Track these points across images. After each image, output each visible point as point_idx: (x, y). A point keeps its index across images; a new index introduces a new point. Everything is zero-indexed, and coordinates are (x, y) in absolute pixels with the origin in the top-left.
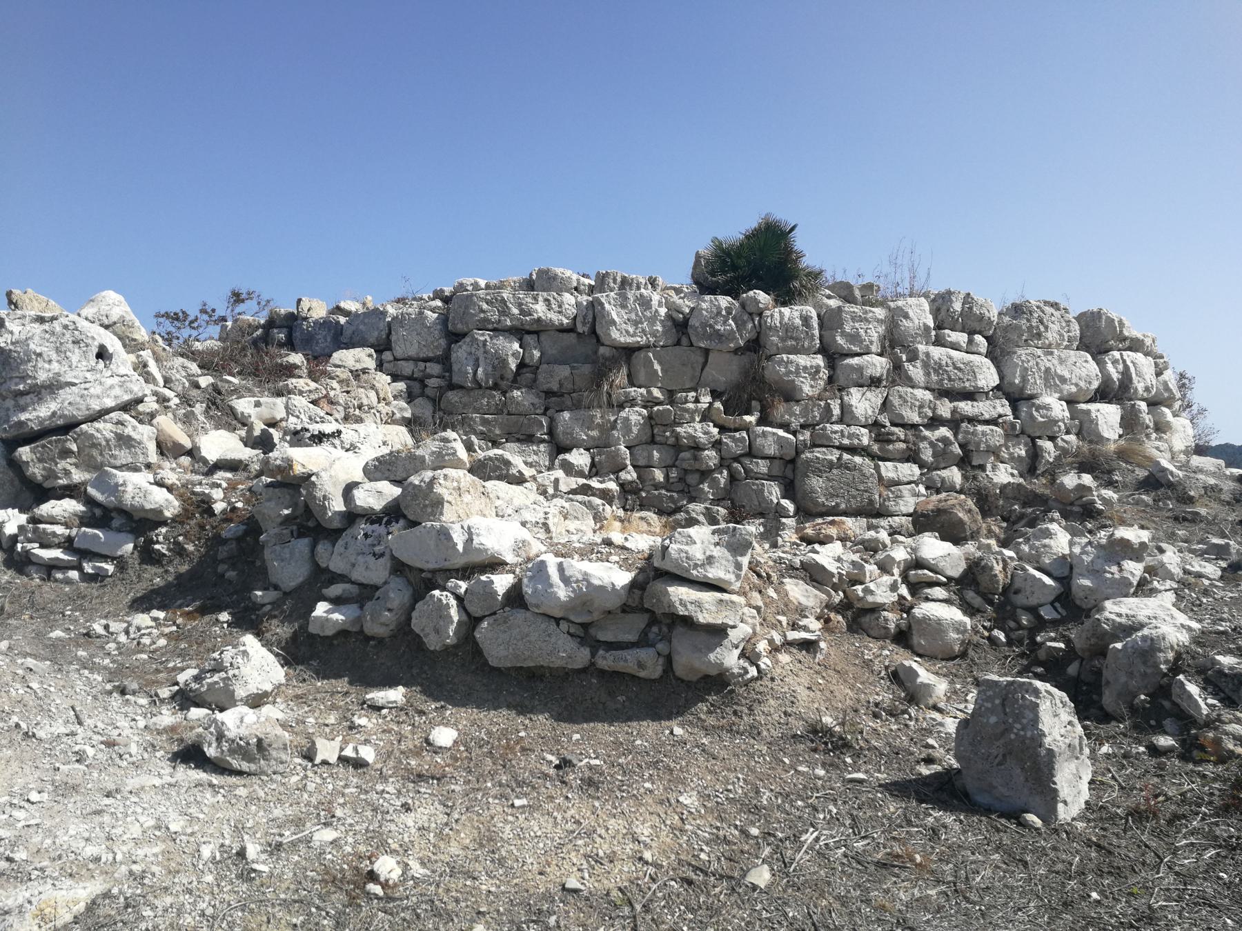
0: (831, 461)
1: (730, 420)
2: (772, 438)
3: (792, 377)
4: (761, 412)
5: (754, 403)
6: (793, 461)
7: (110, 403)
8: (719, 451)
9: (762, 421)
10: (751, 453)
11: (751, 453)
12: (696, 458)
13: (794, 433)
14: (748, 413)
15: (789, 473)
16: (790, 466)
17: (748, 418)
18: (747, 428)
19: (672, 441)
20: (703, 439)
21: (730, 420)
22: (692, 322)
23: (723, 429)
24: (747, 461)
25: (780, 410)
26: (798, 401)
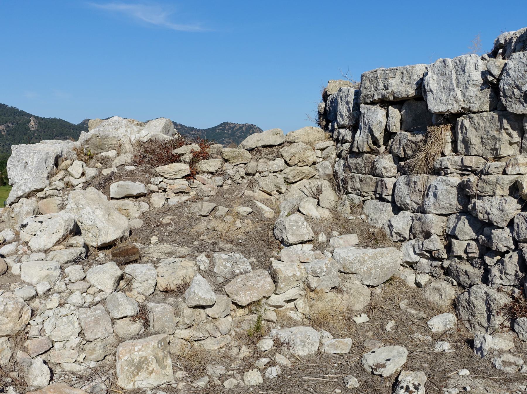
7: (20, 193)
22: (501, 85)
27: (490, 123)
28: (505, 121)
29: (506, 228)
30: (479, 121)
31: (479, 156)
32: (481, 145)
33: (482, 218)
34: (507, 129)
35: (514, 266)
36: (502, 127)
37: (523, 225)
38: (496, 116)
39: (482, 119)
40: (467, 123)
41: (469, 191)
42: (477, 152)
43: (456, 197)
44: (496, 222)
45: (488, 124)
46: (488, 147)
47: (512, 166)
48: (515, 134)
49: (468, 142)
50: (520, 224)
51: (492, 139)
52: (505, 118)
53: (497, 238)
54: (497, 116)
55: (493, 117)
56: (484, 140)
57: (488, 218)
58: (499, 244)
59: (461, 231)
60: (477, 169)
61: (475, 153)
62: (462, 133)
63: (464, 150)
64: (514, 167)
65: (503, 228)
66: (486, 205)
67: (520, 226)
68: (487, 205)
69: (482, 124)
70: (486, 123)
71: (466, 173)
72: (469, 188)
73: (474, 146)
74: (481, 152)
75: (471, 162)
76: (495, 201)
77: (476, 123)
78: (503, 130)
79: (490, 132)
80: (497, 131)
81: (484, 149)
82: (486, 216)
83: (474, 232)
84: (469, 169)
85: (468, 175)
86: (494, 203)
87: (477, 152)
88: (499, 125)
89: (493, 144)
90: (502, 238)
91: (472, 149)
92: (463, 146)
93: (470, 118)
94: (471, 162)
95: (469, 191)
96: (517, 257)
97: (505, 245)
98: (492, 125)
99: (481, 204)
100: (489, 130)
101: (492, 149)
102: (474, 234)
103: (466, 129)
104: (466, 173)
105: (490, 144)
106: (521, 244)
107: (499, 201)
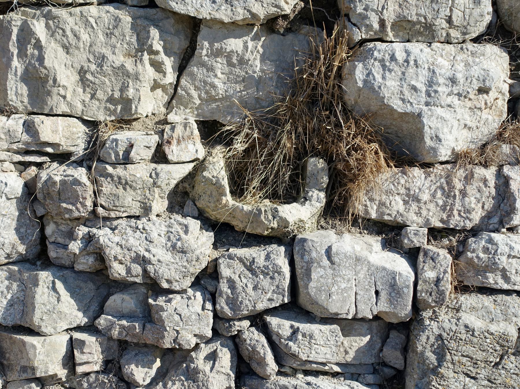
0: (502, 339)
1: (252, 206)
2: (355, 270)
3: (417, 104)
4: (331, 191)
5: (316, 164)
6: (406, 329)
8: (212, 297)
9: (336, 210)
10: (297, 306)
11: (297, 306)
12: (149, 316)
13: (413, 255)
14: (294, 193)
15: (393, 356)
16: (396, 338)
17: (294, 213)
18: (286, 239)
19: (86, 263)
20: (168, 267)
21: (252, 206)
23: (226, 234)
24: (281, 325)
25: (385, 191)
26: (426, 166)
27: (109, 35)
28: (155, 33)
29: (190, 292)
30: (76, 28)
31: (70, 116)
32: (81, 90)
33: (123, 273)
34: (157, 53)
35: (223, 377)
36: (143, 46)
37: (244, 281)
38: (126, 19)
39: (87, 23)
40: (39, 28)
41: (70, 207)
42: (70, 105)
43: (14, 224)
44: (169, 281)
45: (101, 38)
46: (100, 94)
47: (179, 142)
48: (169, 63)
49: (44, 80)
50: (236, 278)
51: (116, 74)
52: (157, 26)
53: (177, 318)
54: (129, 19)
55: (117, 20)
56: (89, 76)
57: (145, 272)
58: (183, 333)
59: (49, 312)
60: (72, 149)
61: (63, 108)
62: (22, 54)
63: (26, 100)
64: (183, 145)
65: (184, 291)
66: (132, 241)
67: (239, 285)
68: (135, 241)
69: (85, 37)
70: (96, 36)
71: (38, 159)
72: (75, 199)
73: (62, 92)
74: (80, 106)
75: (55, 131)
76: (157, 227)
77: (69, 33)
78: (146, 57)
79: (111, 57)
80: (128, 55)
81: (87, 100)
82: (137, 269)
83: (79, 310)
84: (50, 150)
85: (39, 165)
86: (154, 235)
87: (70, 105)
88: (134, 39)
89: (117, 88)
90: (187, 318)
91: (55, 98)
92: (24, 90)
93: (48, 16)
94: (55, 131)
95: (70, 207)
96: (228, 356)
97: (197, 332)
98: (114, 40)
99: (117, 239)
100: (107, 52)
101: (111, 100)
102: (80, 315)
103: (38, 46)
104: (38, 159)
105: (109, 86)
106: (237, 323)
107: (164, 229)
